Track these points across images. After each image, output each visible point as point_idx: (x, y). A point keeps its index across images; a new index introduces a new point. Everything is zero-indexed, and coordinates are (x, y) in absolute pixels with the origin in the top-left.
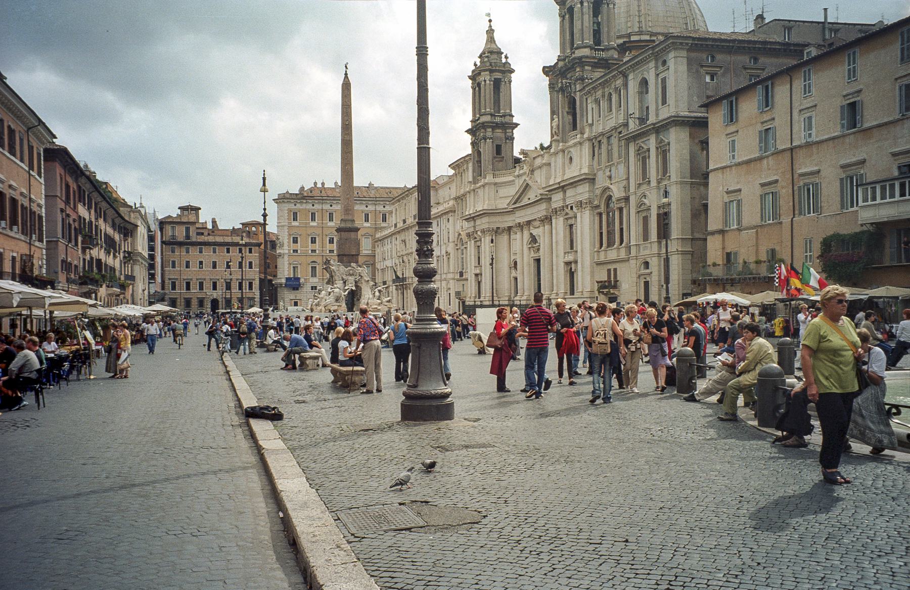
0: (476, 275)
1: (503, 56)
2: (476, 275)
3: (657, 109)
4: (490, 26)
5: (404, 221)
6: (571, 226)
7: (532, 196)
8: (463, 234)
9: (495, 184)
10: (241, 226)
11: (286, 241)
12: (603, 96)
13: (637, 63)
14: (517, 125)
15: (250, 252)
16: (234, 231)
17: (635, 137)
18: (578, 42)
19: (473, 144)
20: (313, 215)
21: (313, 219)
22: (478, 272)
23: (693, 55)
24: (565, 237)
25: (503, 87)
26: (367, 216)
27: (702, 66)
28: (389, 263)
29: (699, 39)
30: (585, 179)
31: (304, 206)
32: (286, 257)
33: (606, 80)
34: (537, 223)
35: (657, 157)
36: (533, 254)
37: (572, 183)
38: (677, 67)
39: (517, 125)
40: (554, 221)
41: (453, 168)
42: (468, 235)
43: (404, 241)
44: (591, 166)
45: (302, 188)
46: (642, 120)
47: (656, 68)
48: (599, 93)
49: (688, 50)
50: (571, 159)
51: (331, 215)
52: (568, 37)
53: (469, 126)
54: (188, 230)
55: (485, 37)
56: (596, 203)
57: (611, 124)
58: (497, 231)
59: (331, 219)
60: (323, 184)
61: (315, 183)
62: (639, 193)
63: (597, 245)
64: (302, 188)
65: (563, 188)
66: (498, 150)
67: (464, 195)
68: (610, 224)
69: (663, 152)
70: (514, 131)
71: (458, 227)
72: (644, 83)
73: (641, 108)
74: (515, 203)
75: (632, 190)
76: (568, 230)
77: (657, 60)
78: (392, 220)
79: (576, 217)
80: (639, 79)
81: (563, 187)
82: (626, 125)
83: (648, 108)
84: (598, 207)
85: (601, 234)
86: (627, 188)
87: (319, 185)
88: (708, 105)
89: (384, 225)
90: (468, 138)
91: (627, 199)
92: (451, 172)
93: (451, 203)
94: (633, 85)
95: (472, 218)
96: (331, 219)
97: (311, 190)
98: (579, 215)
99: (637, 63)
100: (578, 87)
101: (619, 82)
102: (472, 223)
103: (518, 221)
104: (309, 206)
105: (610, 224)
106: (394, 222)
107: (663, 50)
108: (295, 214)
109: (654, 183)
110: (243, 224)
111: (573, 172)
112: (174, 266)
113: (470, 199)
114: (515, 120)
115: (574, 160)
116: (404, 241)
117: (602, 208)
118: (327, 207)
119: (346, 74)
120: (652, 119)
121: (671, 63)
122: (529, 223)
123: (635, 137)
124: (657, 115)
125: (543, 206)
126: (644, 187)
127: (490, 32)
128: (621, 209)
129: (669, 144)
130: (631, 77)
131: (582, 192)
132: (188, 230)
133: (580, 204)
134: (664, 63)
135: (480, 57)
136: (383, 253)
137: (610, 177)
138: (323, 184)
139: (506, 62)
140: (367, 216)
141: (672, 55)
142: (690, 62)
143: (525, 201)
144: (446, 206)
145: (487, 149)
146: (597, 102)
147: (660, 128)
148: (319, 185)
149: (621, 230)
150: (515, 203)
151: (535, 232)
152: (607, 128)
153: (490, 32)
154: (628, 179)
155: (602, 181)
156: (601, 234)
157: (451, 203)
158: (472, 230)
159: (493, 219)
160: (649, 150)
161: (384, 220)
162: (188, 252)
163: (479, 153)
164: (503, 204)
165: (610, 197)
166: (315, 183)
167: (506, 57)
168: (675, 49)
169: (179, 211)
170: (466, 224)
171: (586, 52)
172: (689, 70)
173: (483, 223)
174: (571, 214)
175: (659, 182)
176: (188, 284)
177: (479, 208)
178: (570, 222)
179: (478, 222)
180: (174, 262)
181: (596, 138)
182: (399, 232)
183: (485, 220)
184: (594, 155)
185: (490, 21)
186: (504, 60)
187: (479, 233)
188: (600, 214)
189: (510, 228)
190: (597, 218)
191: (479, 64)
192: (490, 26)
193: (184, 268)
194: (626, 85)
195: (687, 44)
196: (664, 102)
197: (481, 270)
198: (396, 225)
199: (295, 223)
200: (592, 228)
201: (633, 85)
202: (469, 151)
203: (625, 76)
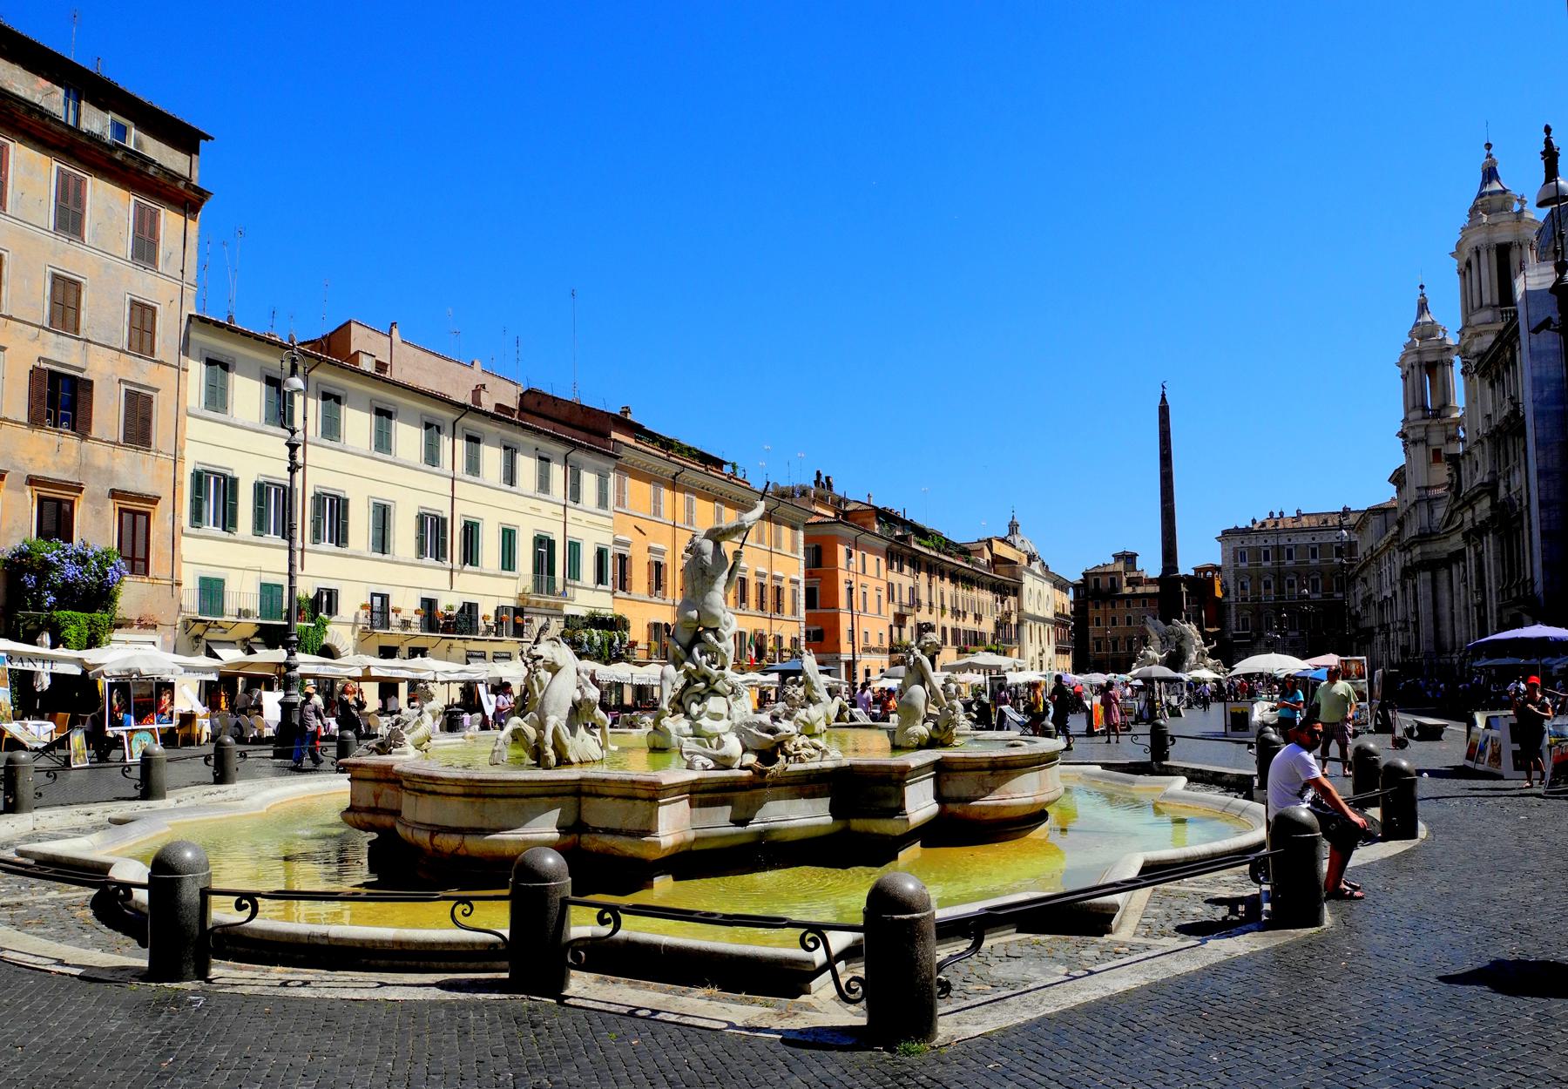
10: (1192, 573)
20: (1266, 553)
21: (1267, 559)
25: (1439, 369)
32: (1233, 609)
44: (1492, 472)
45: (1254, 522)
51: (1290, 552)
53: (1399, 427)
60: (1281, 514)
61: (1271, 514)
74: (1447, 525)
87: (1276, 515)
93: (1396, 528)
96: (1290, 557)
97: (1263, 524)
108: (1243, 555)
116: (1365, 580)
132: (1113, 580)
138: (1281, 514)
148: (1276, 515)
150: (1447, 525)
155: (1502, 492)
159: (1428, 548)
166: (1271, 514)
169: (1112, 561)
183: (1417, 550)
199: (1243, 565)
202: (1401, 460)
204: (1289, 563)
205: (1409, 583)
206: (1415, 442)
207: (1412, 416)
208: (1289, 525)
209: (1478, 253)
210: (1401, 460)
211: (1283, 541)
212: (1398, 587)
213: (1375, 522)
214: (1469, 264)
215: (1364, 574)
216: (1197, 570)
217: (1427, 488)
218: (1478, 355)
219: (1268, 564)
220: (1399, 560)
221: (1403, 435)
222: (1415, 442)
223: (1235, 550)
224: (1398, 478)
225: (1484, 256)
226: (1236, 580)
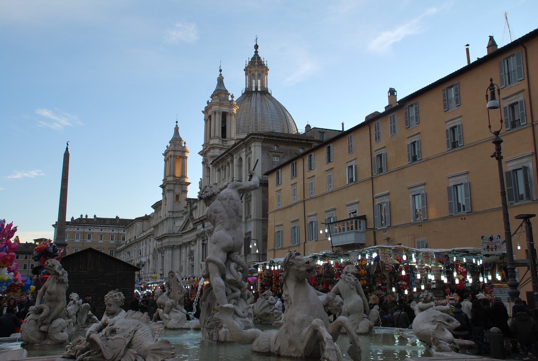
0: (161, 275)
2: (161, 275)
4: (177, 125)
5: (130, 240)
7: (191, 226)
8: (156, 249)
9: (174, 218)
12: (222, 167)
14: (189, 183)
18: (212, 135)
19: (163, 194)
21: (77, 238)
22: (162, 273)
23: (265, 145)
26: (112, 236)
29: (268, 136)
31: (72, 230)
34: (193, 243)
35: (245, 204)
36: (191, 262)
38: (256, 150)
39: (189, 183)
40: (198, 242)
41: (154, 208)
42: (159, 250)
43: (129, 253)
45: (73, 218)
47: (246, 151)
48: (220, 165)
49: (262, 142)
52: (208, 133)
55: (173, 131)
58: (173, 248)
59: (89, 238)
60: (87, 216)
61: (82, 216)
64: (73, 218)
65: (202, 221)
66: (177, 197)
67: (158, 225)
70: (188, 187)
71: (155, 245)
72: (241, 159)
77: (246, 147)
78: (127, 239)
80: (238, 157)
81: (202, 221)
88: (268, 174)
89: (123, 242)
90: (161, 189)
93: (152, 229)
95: (160, 239)
96: (89, 238)
98: (209, 238)
101: (229, 159)
102: (160, 243)
103: (184, 241)
104: (76, 230)
109: (243, 220)
110: (35, 240)
113: (160, 227)
114: (187, 180)
116: (129, 253)
118: (87, 230)
121: (252, 149)
122: (189, 243)
125: (195, 233)
127: (177, 129)
129: (251, 196)
130: (235, 157)
134: (250, 148)
135: (170, 142)
138: (87, 216)
139: (185, 146)
140: (112, 236)
141: (253, 145)
142: (263, 149)
143: (188, 229)
144: (149, 231)
145: (170, 196)
146: (219, 170)
150: (182, 231)
151: (192, 248)
153: (177, 129)
157: (152, 229)
158: (160, 246)
159: (171, 240)
163: (166, 198)
164: (176, 230)
166: (82, 216)
167: (185, 143)
168: (255, 141)
170: (159, 243)
171: (216, 141)
172: (263, 153)
173: (166, 241)
174: (205, 238)
175: (246, 218)
179: (164, 242)
183: (167, 240)
185: (177, 122)
186: (183, 145)
189: (180, 245)
192: (177, 125)
194: (232, 161)
195: (261, 138)
197: (163, 272)
201: (235, 161)
202: (160, 198)
204: (89, 241)
205: (160, 255)
206: (169, 191)
207: (169, 179)
209: (215, 113)
210: (160, 198)
211: (87, 230)
212: (151, 257)
213: (139, 224)
214: (210, 117)
215: (128, 250)
216: (36, 241)
217: (173, 212)
220: (153, 244)
221: (162, 186)
222: (169, 191)
224: (157, 206)
225: (217, 115)
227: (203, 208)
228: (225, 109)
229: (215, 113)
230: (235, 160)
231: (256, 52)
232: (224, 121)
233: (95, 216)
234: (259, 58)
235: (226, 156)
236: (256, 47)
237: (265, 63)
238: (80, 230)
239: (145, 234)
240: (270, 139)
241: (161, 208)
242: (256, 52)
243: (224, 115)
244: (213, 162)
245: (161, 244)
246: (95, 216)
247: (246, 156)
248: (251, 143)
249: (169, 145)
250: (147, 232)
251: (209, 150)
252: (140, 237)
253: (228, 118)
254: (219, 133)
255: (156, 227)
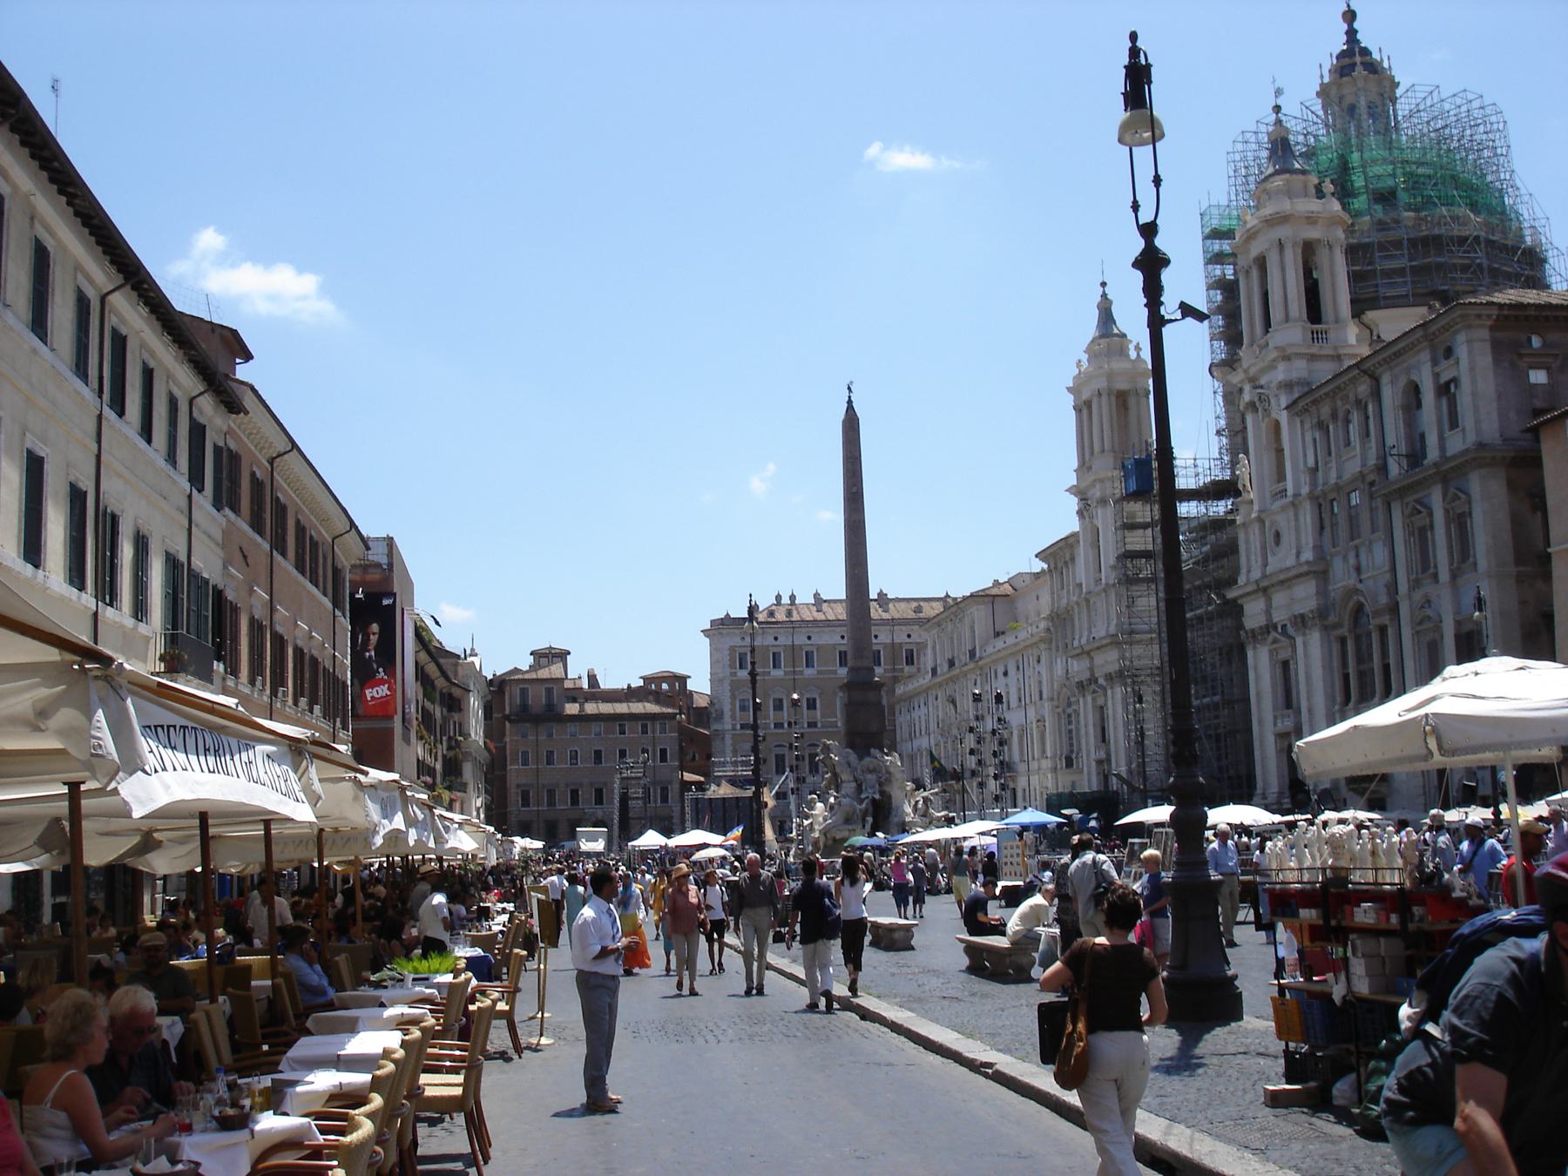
1: (1132, 347)
3: (1441, 438)
4: (1104, 295)
6: (1285, 665)
11: (727, 709)
12: (1334, 416)
13: (1398, 354)
15: (663, 731)
16: (630, 694)
17: (1402, 492)
19: (1080, 513)
22: (1103, 755)
24: (1274, 686)
25: (1132, 401)
27: (1521, 356)
28: (923, 742)
30: (1307, 573)
32: (728, 741)
33: (1338, 388)
37: (1282, 582)
40: (1250, 654)
44: (1318, 548)
46: (1415, 456)
47: (1435, 362)
50: (1278, 535)
54: (549, 691)
55: (1094, 314)
56: (1332, 619)
57: (1353, 467)
60: (793, 597)
61: (778, 597)
62: (1418, 596)
63: (1339, 699)
68: (1363, 657)
69: (1460, 523)
71: (1059, 670)
72: (1415, 389)
73: (1410, 437)
75: (1403, 587)
76: (1279, 671)
77: (1433, 349)
79: (1294, 647)
80: (1402, 381)
81: (1265, 590)
82: (1383, 468)
83: (1422, 436)
84: (1338, 625)
85: (1346, 677)
86: (1393, 587)
87: (786, 600)
90: (1073, 503)
91: (1394, 609)
92: (1039, 566)
94: (1391, 395)
98: (1299, 641)
99: (1398, 354)
100: (1284, 403)
102: (1086, 663)
105: (1363, 657)
106: (930, 665)
107: (1446, 328)
109: (1444, 576)
111: (1283, 559)
112: (525, 763)
115: (1285, 539)
117: (1344, 631)
119: (850, 402)
120: (1433, 454)
121: (1462, 351)
123: (1402, 492)
124: (1442, 448)
126: (1428, 588)
128: (1383, 630)
130: (1385, 379)
131: (1304, 597)
132: (549, 691)
133: (1301, 621)
134: (1449, 352)
136: (912, 725)
137: (1358, 569)
138: (793, 597)
141: (1461, 338)
142: (1496, 346)
146: (1322, 426)
147: (1451, 474)
148: (786, 600)
149: (1386, 668)
152: (1347, 476)
154: (1393, 569)
155: (1342, 577)
156: (1346, 677)
160: (1431, 514)
161: (910, 660)
162: (550, 735)
165: (1359, 609)
166: (778, 597)
168: (1469, 327)
172: (1497, 362)
176: (551, 793)
177: (1100, 631)
178: (1283, 655)
180: (525, 754)
181: (1324, 494)
182: (940, 685)
184: (1322, 528)
185: (1104, 284)
187: (1101, 681)
188: (1343, 641)
190: (1336, 647)
191: (1085, 364)
192: (1104, 295)
193: (543, 765)
194: (1376, 394)
195: (1489, 316)
196: (1454, 423)
198: (934, 671)
200: (1327, 667)
201: (1391, 395)
202: (1072, 524)
203: (1376, 380)
204: (809, 672)
206: (1103, 502)
208: (807, 616)
210: (1072, 524)
211: (800, 640)
218: (1288, 386)
219: (778, 673)
223: (732, 649)
224: (1058, 555)
226: (733, 697)
227: (1264, 548)
228: (1313, 233)
229: (1281, 245)
230: (1387, 393)
231: (1351, 34)
232: (1308, 272)
233: (816, 596)
234: (1365, 52)
235: (1350, 380)
236: (1350, 16)
237: (1386, 65)
238: (782, 640)
239: (1010, 640)
240: (1516, 317)
241: (1073, 559)
242: (1351, 34)
243: (1309, 249)
244: (1295, 402)
245: (1091, 669)
246: (816, 596)
247: (1436, 376)
248: (1456, 332)
249: (1084, 358)
250: (1022, 635)
251: (1272, 366)
252: (990, 650)
253: (1322, 257)
254: (1298, 306)
255: (1060, 620)
